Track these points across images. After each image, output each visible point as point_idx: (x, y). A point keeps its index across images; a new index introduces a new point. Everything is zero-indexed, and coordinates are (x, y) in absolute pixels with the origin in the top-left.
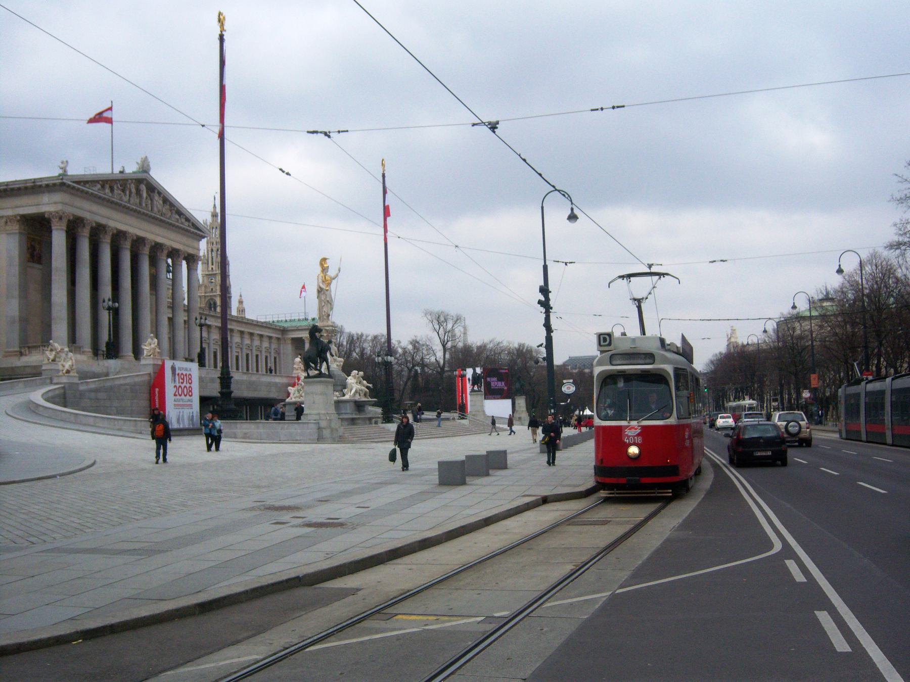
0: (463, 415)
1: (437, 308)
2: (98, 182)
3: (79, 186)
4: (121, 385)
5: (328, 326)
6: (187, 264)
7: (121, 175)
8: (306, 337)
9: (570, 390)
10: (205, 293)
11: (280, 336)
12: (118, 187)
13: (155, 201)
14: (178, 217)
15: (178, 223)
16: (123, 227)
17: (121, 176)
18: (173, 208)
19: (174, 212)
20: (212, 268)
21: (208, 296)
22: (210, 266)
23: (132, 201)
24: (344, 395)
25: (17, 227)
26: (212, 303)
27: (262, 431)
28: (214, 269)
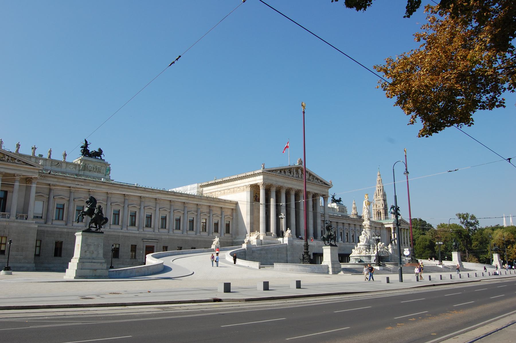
0: (441, 263)
2: (278, 170)
3: (270, 172)
7: (289, 167)
8: (392, 227)
9: (408, 253)
11: (380, 227)
14: (316, 180)
15: (316, 182)
17: (289, 167)
19: (315, 178)
23: (294, 176)
25: (250, 189)
26: (379, 212)
27: (298, 268)
28: (380, 198)
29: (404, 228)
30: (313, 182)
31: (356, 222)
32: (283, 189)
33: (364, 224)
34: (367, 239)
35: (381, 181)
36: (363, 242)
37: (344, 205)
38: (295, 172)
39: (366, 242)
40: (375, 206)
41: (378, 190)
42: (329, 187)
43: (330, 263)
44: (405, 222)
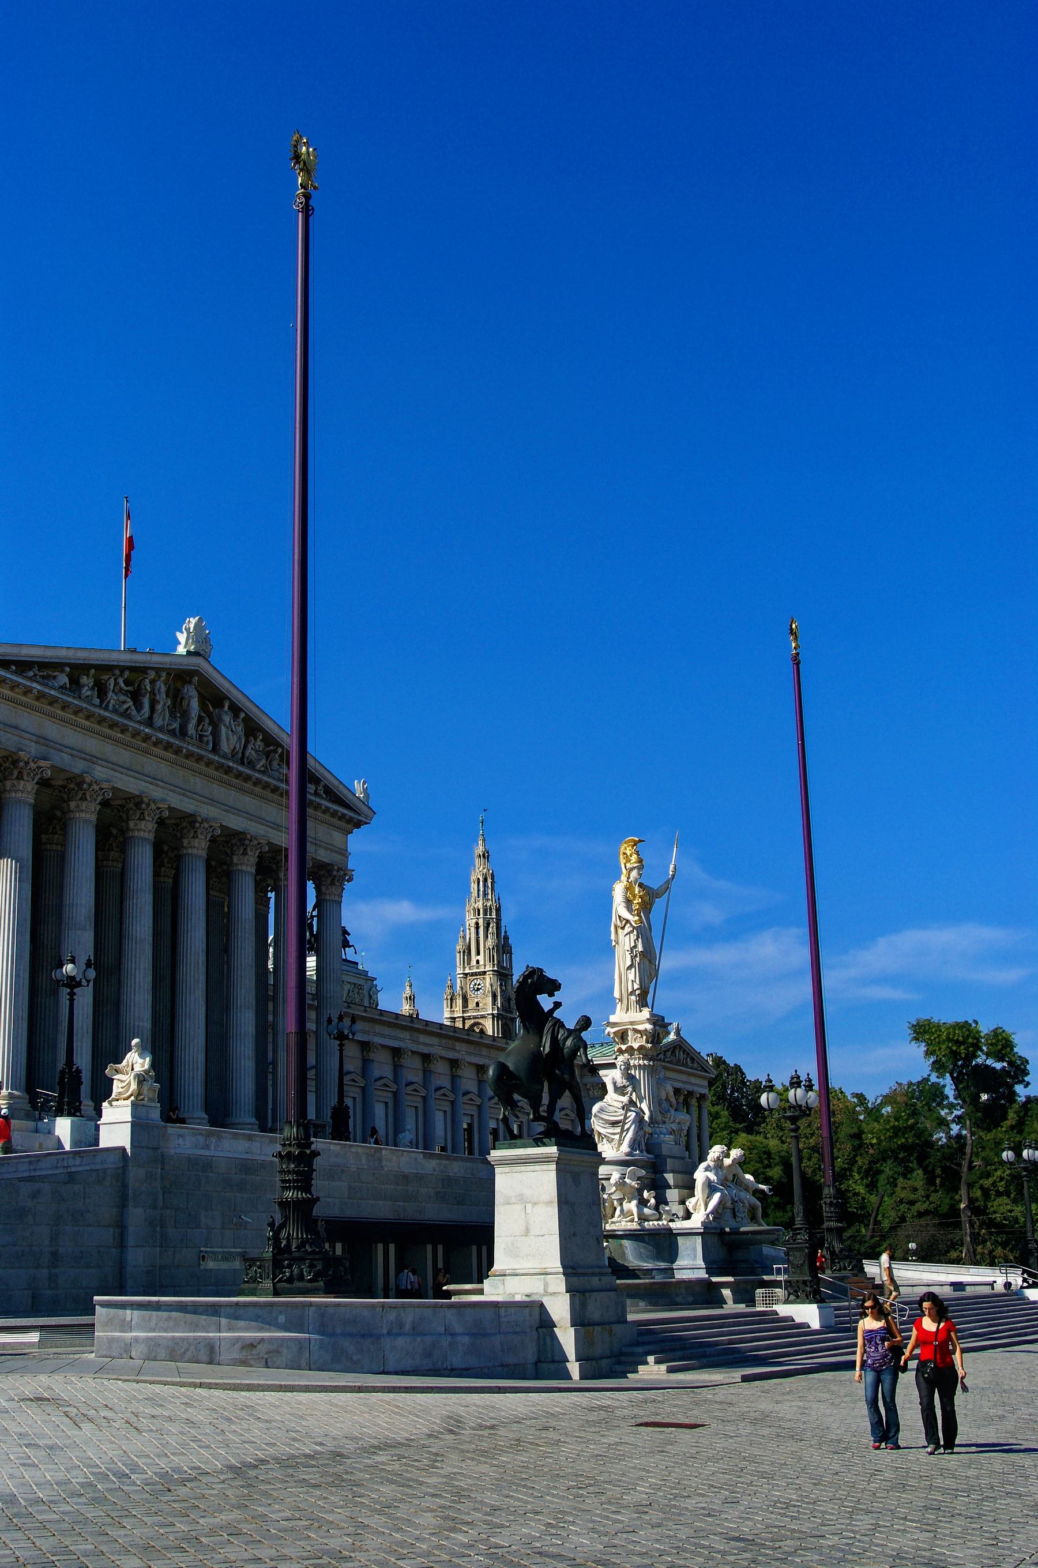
1: (947, 1015)
2: (58, 666)
4: (22, 1179)
5: (641, 1023)
6: (318, 889)
10: (463, 1012)
12: (116, 684)
13: (223, 730)
16: (131, 785)
17: (126, 659)
18: (271, 748)
20: (478, 962)
21: (469, 1018)
22: (474, 958)
23: (158, 721)
24: (688, 1215)
28: (482, 962)
29: (690, 1088)
30: (265, 778)
31: (458, 1046)
32: (83, 798)
33: (614, 1025)
34: (639, 1120)
35: (489, 881)
36: (620, 1144)
37: (360, 967)
38: (162, 697)
39: (634, 1145)
40: (459, 1002)
41: (477, 924)
42: (350, 821)
43: (559, 1284)
44: (693, 1060)
